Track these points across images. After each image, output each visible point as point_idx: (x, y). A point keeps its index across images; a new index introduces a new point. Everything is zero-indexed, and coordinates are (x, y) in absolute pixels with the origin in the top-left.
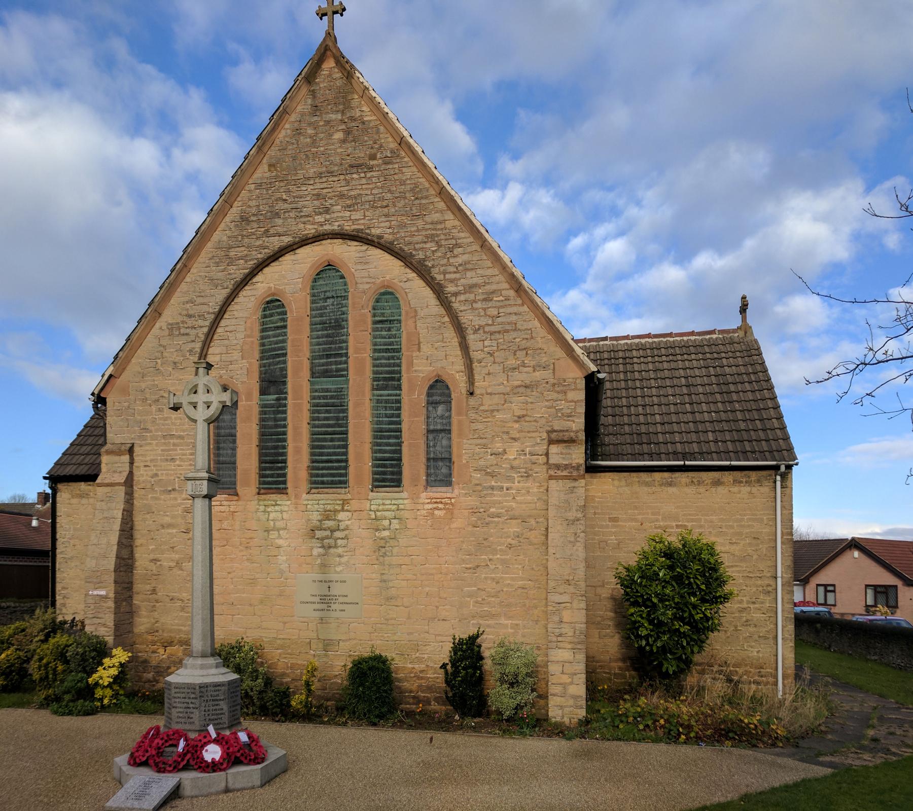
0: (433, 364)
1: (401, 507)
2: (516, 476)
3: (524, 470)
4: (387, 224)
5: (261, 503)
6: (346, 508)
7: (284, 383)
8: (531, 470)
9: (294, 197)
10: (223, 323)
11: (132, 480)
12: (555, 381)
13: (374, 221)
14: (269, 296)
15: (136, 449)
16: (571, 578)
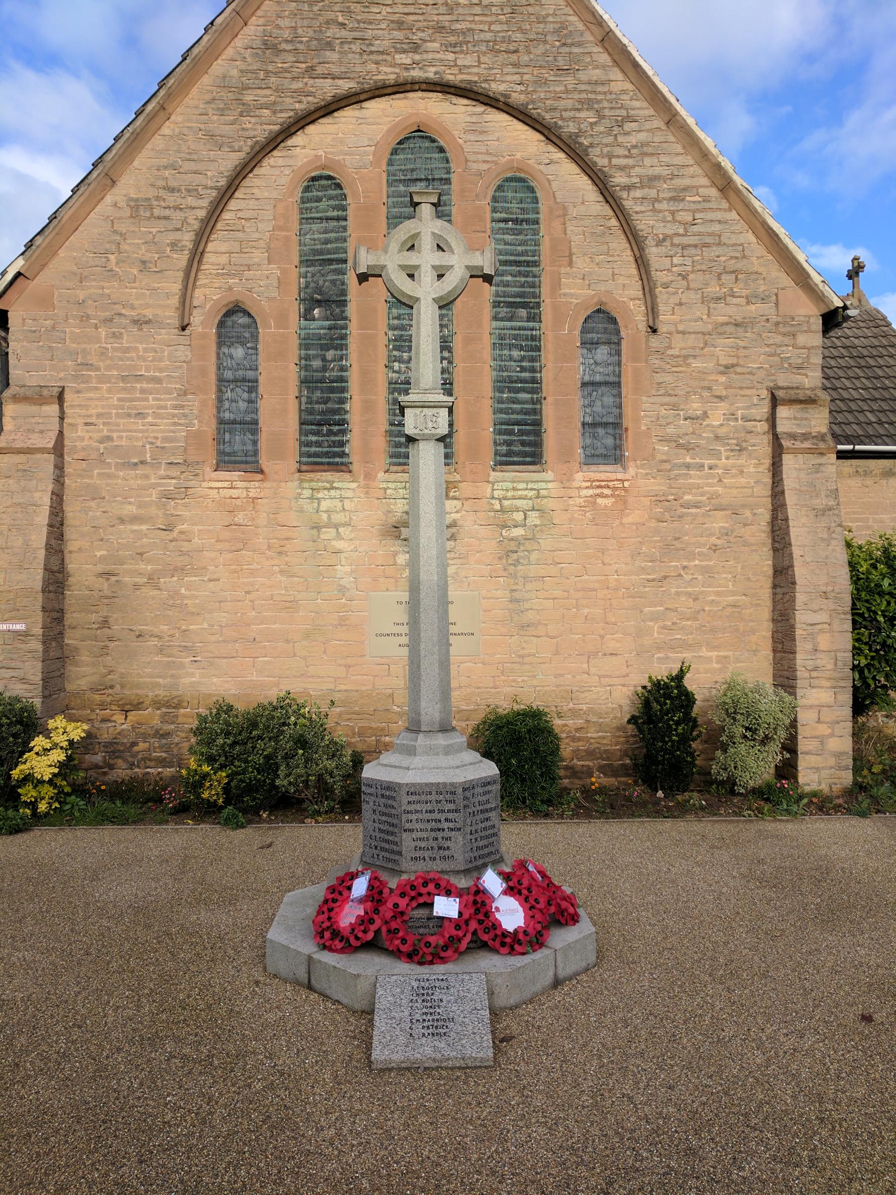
0: (593, 286)
1: (543, 492)
2: (722, 449)
3: (734, 441)
4: (517, 78)
5: (306, 485)
6: (451, 494)
7: (343, 303)
8: (745, 441)
9: (358, 22)
10: (233, 205)
11: (63, 446)
12: (779, 319)
13: (496, 71)
14: (316, 168)
15: (68, 396)
16: (830, 588)
